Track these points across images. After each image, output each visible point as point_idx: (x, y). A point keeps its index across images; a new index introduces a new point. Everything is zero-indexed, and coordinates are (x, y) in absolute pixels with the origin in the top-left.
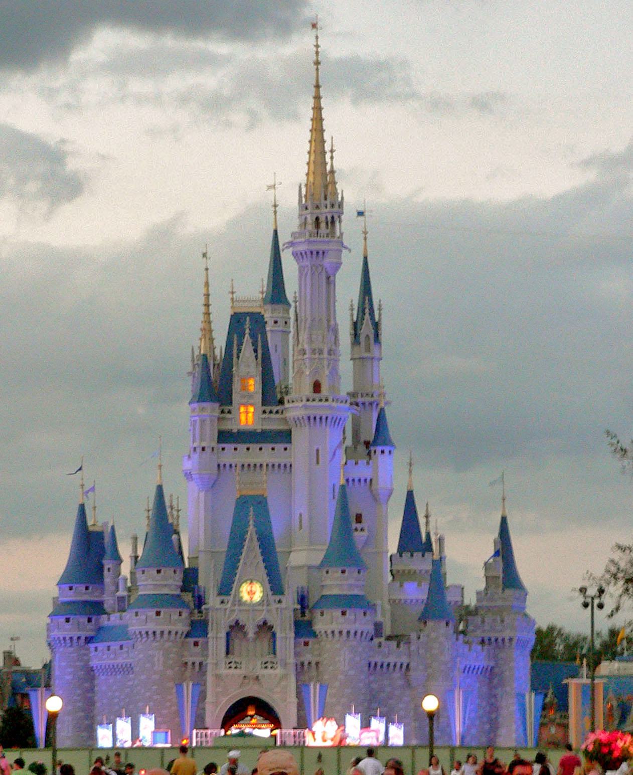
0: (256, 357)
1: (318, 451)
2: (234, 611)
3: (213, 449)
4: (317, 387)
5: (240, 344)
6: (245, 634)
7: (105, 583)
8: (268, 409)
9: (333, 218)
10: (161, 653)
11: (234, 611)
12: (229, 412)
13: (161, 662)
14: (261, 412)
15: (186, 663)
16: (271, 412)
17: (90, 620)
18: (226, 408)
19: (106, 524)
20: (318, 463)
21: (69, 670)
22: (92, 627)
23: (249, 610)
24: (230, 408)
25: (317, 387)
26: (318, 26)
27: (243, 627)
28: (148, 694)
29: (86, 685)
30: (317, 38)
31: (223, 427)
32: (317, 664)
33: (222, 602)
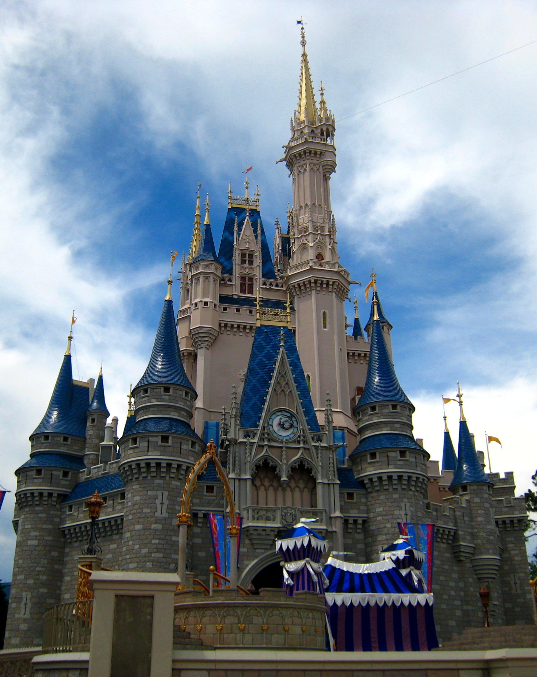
0: (256, 237)
1: (324, 314)
2: (263, 446)
3: (215, 305)
4: (320, 256)
5: (241, 224)
6: (278, 477)
7: (88, 437)
8: (268, 281)
9: (327, 129)
10: (166, 493)
11: (263, 446)
12: (230, 280)
13: (165, 507)
14: (261, 283)
15: (197, 514)
16: (271, 284)
17: (65, 474)
18: (227, 277)
19: (92, 380)
20: (325, 327)
21: (33, 534)
22: (68, 483)
23: (282, 447)
24: (230, 276)
25: (320, 256)
26: (303, 22)
27: (274, 468)
28: (144, 551)
29: (55, 554)
30: (302, 28)
31: (220, 293)
32: (364, 522)
33: (247, 435)
